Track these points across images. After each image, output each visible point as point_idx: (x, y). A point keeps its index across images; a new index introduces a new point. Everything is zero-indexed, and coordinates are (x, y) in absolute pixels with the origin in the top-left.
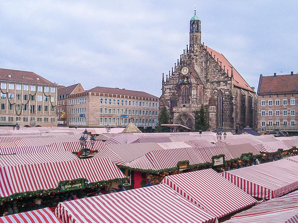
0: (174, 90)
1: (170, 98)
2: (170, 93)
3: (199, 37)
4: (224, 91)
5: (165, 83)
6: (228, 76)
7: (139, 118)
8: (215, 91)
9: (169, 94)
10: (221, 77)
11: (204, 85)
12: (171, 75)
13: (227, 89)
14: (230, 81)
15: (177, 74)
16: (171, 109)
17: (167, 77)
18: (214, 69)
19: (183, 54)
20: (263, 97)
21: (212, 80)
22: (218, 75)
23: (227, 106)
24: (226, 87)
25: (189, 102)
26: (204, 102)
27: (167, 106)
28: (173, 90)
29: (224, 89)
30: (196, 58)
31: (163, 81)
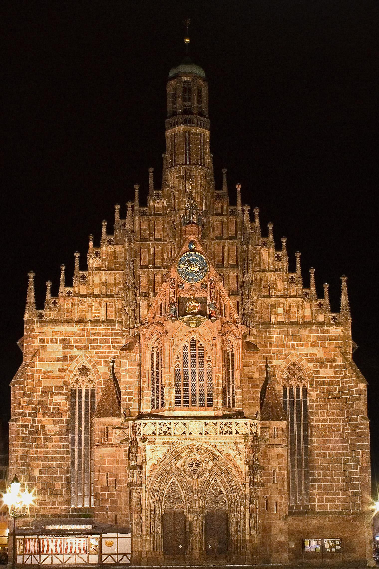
0: (86, 348)
1: (66, 383)
2: (64, 360)
4: (316, 367)
8: (275, 362)
13: (328, 360)
16: (67, 434)
21: (261, 317)
23: (329, 426)
24: (325, 349)
25: (210, 399)
27: (51, 416)
28: (79, 349)
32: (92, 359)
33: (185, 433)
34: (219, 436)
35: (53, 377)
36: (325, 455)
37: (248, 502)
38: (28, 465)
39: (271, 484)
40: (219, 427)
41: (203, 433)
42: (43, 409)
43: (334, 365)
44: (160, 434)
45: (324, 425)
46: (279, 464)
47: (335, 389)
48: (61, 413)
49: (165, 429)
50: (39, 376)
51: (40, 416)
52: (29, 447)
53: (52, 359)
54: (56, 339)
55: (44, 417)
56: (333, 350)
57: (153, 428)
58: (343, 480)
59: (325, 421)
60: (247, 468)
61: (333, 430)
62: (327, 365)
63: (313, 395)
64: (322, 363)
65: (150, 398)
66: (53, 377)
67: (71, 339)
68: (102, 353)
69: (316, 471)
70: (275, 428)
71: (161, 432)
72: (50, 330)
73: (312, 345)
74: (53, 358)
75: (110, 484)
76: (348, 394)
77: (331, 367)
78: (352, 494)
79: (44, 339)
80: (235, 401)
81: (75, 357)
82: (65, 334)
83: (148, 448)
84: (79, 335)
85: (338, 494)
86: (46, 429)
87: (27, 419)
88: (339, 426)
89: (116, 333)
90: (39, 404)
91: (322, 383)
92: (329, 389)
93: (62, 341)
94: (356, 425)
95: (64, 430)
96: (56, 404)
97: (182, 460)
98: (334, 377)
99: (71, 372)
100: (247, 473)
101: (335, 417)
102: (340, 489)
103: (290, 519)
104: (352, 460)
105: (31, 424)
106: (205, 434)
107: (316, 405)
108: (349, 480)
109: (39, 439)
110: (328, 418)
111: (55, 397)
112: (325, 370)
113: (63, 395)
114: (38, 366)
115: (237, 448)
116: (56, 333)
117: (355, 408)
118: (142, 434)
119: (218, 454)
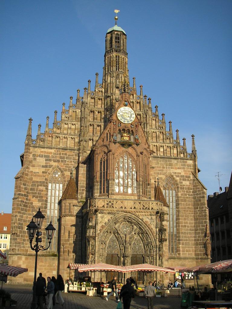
0: (58, 161)
1: (46, 179)
2: (46, 166)
4: (180, 179)
5: (34, 142)
6: (184, 151)
8: (160, 176)
10: (172, 150)
15: (66, 126)
18: (157, 133)
19: (87, 88)
22: (167, 145)
23: (187, 211)
27: (37, 197)
28: (55, 161)
31: (29, 136)
32: (61, 167)
33: (122, 207)
34: (142, 210)
35: (39, 176)
36: (185, 226)
37: (158, 250)
38: (22, 224)
40: (142, 205)
41: (133, 208)
42: (33, 193)
43: (189, 180)
44: (107, 207)
45: (184, 211)
47: (190, 192)
48: (42, 196)
50: (31, 175)
51: (30, 197)
52: (23, 214)
53: (39, 166)
54: (42, 155)
55: (33, 197)
56: (189, 172)
57: (103, 204)
58: (195, 240)
59: (185, 208)
60: (157, 230)
61: (189, 213)
62: (186, 179)
63: (180, 194)
64: (184, 178)
65: (99, 187)
66: (39, 176)
67: (51, 155)
68: (67, 164)
69: (181, 235)
71: (108, 206)
72: (39, 150)
73: (178, 168)
74: (40, 165)
75: (71, 237)
76: (197, 194)
77: (188, 180)
78: (200, 248)
80: (147, 192)
81: (52, 165)
82: (47, 153)
83: (99, 215)
84: (55, 154)
85: (192, 247)
86: (34, 204)
87: (23, 198)
88: (192, 211)
89: (75, 155)
90: (30, 190)
91: (183, 189)
92: (187, 192)
93: (45, 156)
94: (203, 210)
95: (44, 206)
96: (40, 191)
97: (119, 224)
98: (189, 186)
99: (49, 174)
100: (158, 233)
101: (190, 206)
102: (193, 245)
103: (169, 260)
104: (200, 229)
105: (25, 201)
106: (134, 208)
107: (181, 200)
108: (198, 240)
109: (29, 210)
110: (187, 207)
111: (39, 187)
113: (44, 186)
114: (31, 169)
115: (151, 218)
116: (42, 152)
117: (202, 202)
118: (96, 206)
119: (141, 221)
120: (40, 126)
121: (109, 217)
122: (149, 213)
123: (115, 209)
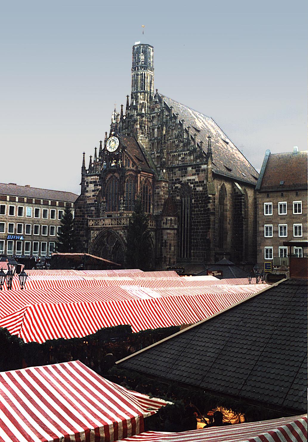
3: (147, 78)
4: (194, 186)
5: (88, 172)
7: (49, 241)
8: (176, 185)
9: (93, 193)
11: (153, 174)
12: (98, 157)
14: (205, 164)
17: (91, 160)
20: (268, 197)
22: (183, 153)
23: (200, 217)
24: (198, 177)
26: (153, 208)
29: (194, 181)
30: (142, 121)
31: (83, 167)
33: (104, 224)
39: (163, 247)
44: (95, 225)
46: (167, 237)
49: (97, 223)
52: (80, 230)
54: (92, 182)
57: (92, 223)
59: (198, 214)
61: (201, 219)
62: (199, 185)
66: (91, 199)
70: (166, 220)
77: (202, 186)
79: (88, 182)
83: (92, 232)
96: (91, 211)
98: (203, 191)
112: (199, 188)
116: (92, 179)
120: (91, 157)
121: (98, 232)
122: (122, 228)
123: (99, 226)
